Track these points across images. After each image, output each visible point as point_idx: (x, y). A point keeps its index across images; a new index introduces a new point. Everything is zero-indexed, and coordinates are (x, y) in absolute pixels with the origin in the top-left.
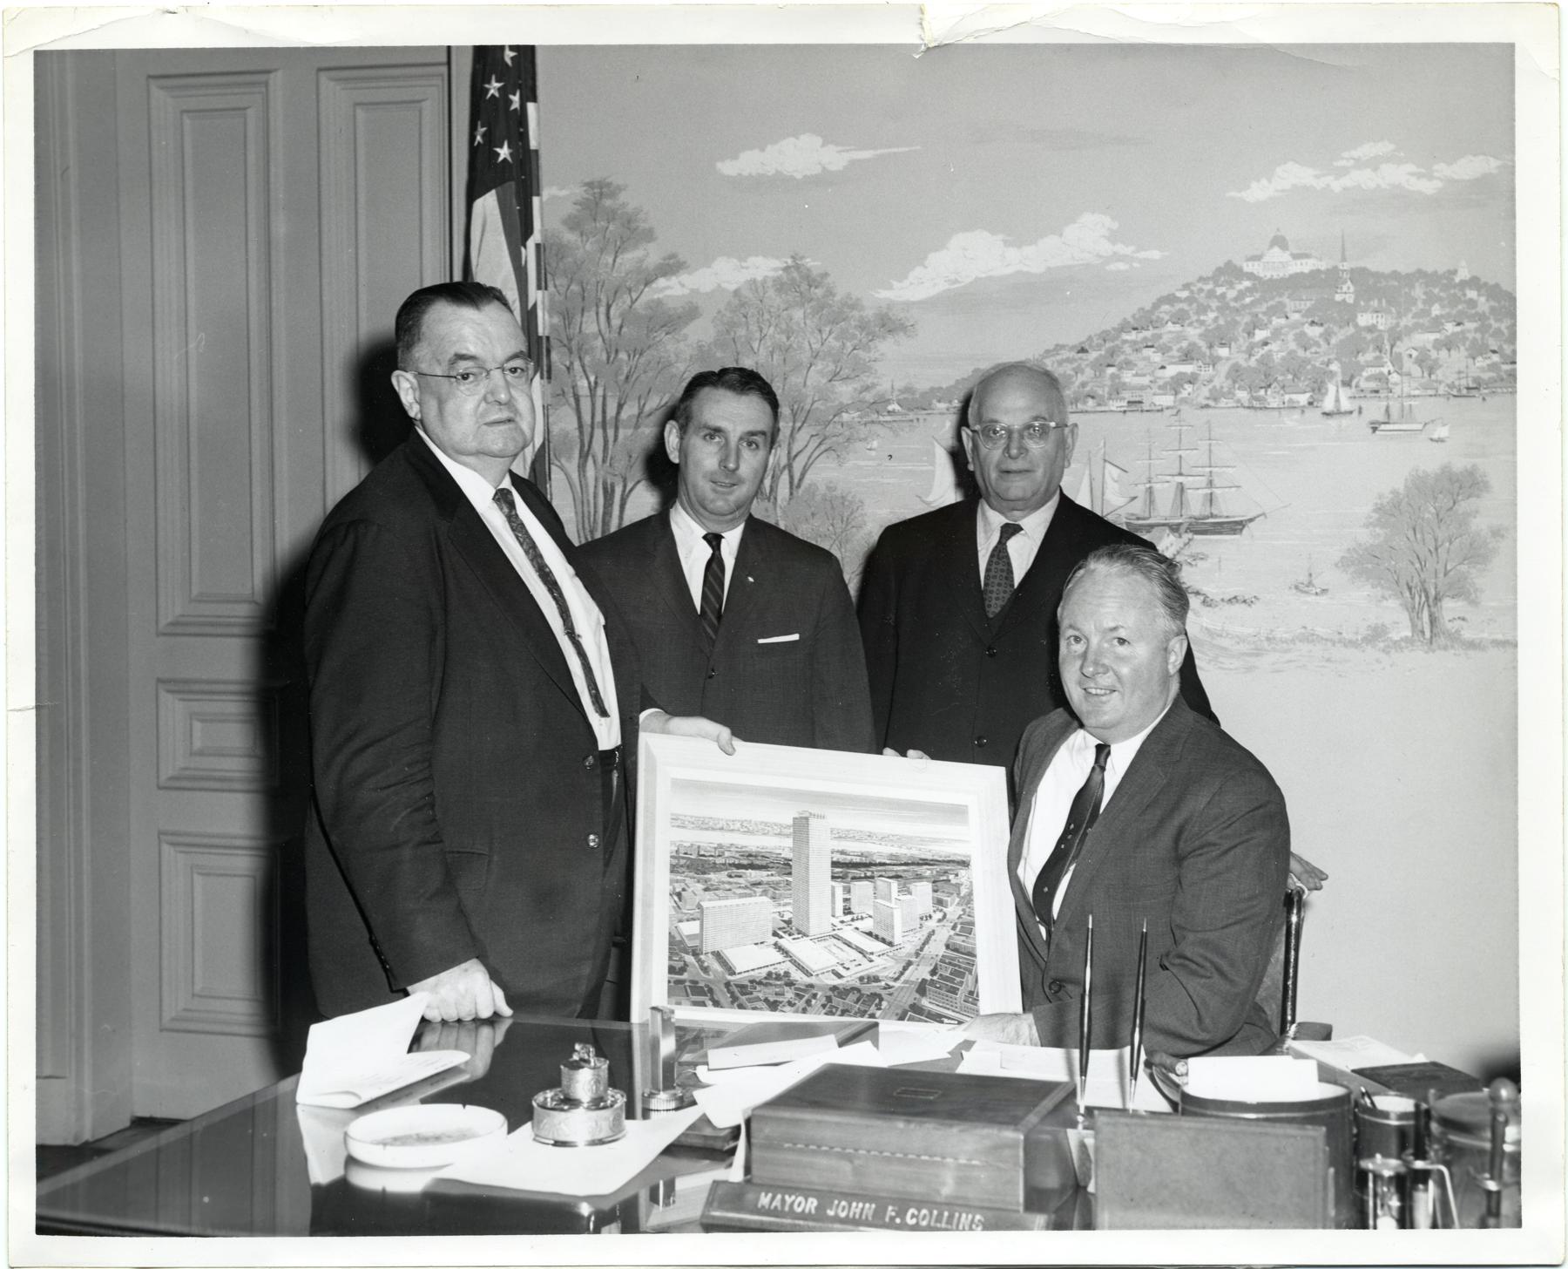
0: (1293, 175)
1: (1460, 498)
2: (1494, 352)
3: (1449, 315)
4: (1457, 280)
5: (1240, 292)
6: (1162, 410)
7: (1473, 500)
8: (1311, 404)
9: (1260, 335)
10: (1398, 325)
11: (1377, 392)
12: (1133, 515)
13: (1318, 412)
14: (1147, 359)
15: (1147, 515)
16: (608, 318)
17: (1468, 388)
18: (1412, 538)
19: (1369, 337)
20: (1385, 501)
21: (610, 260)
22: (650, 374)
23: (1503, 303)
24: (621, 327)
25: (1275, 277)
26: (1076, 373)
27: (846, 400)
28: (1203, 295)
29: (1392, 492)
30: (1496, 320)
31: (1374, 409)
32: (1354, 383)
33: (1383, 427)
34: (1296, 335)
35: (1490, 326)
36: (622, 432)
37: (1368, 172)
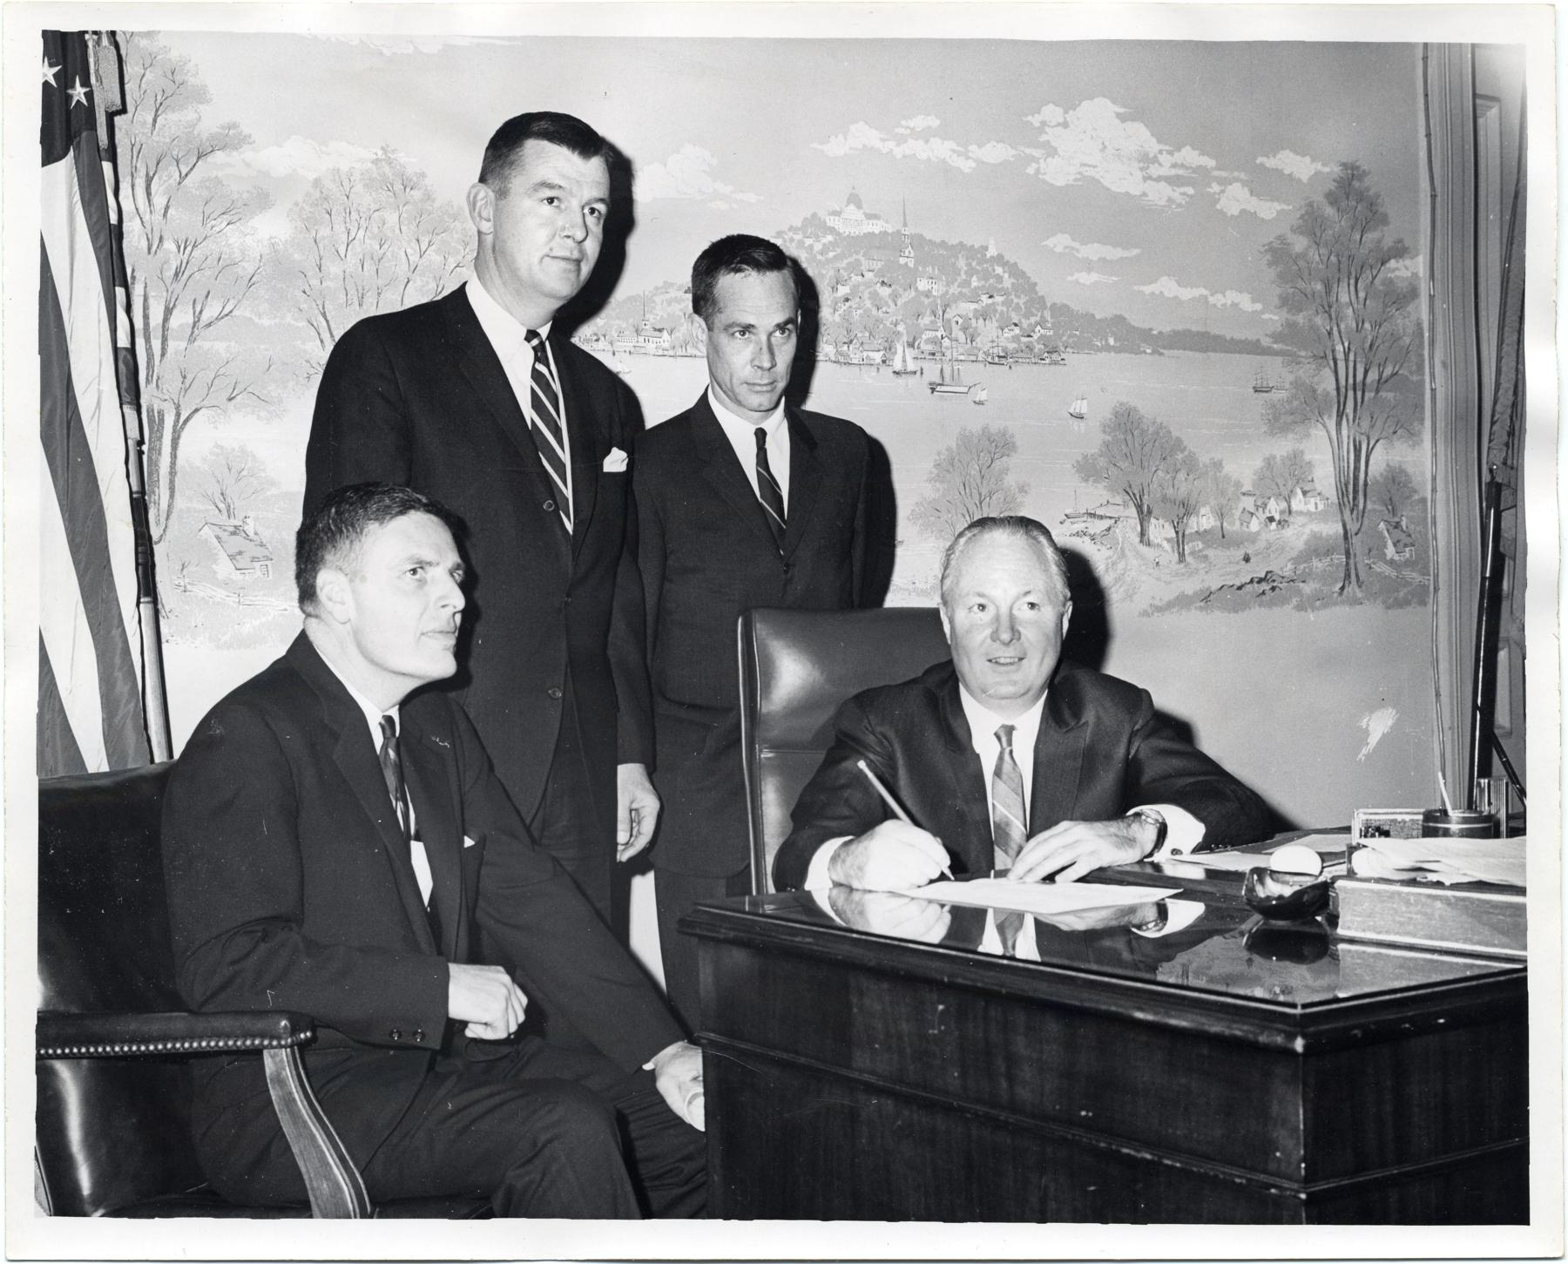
0: (865, 135)
1: (996, 456)
2: (1016, 325)
3: (984, 286)
4: (988, 256)
5: (824, 245)
7: (1005, 458)
8: (884, 362)
9: (843, 291)
10: (947, 292)
11: (934, 354)
13: (890, 370)
16: (149, 194)
17: (999, 357)
18: (963, 493)
19: (926, 301)
20: (943, 457)
21: (150, 119)
22: (208, 273)
23: (1020, 281)
24: (167, 208)
25: (852, 234)
28: (793, 244)
29: (947, 450)
30: (1016, 296)
31: (932, 372)
32: (916, 344)
33: (939, 388)
34: (870, 293)
35: (1012, 300)
36: (171, 345)
37: (921, 142)
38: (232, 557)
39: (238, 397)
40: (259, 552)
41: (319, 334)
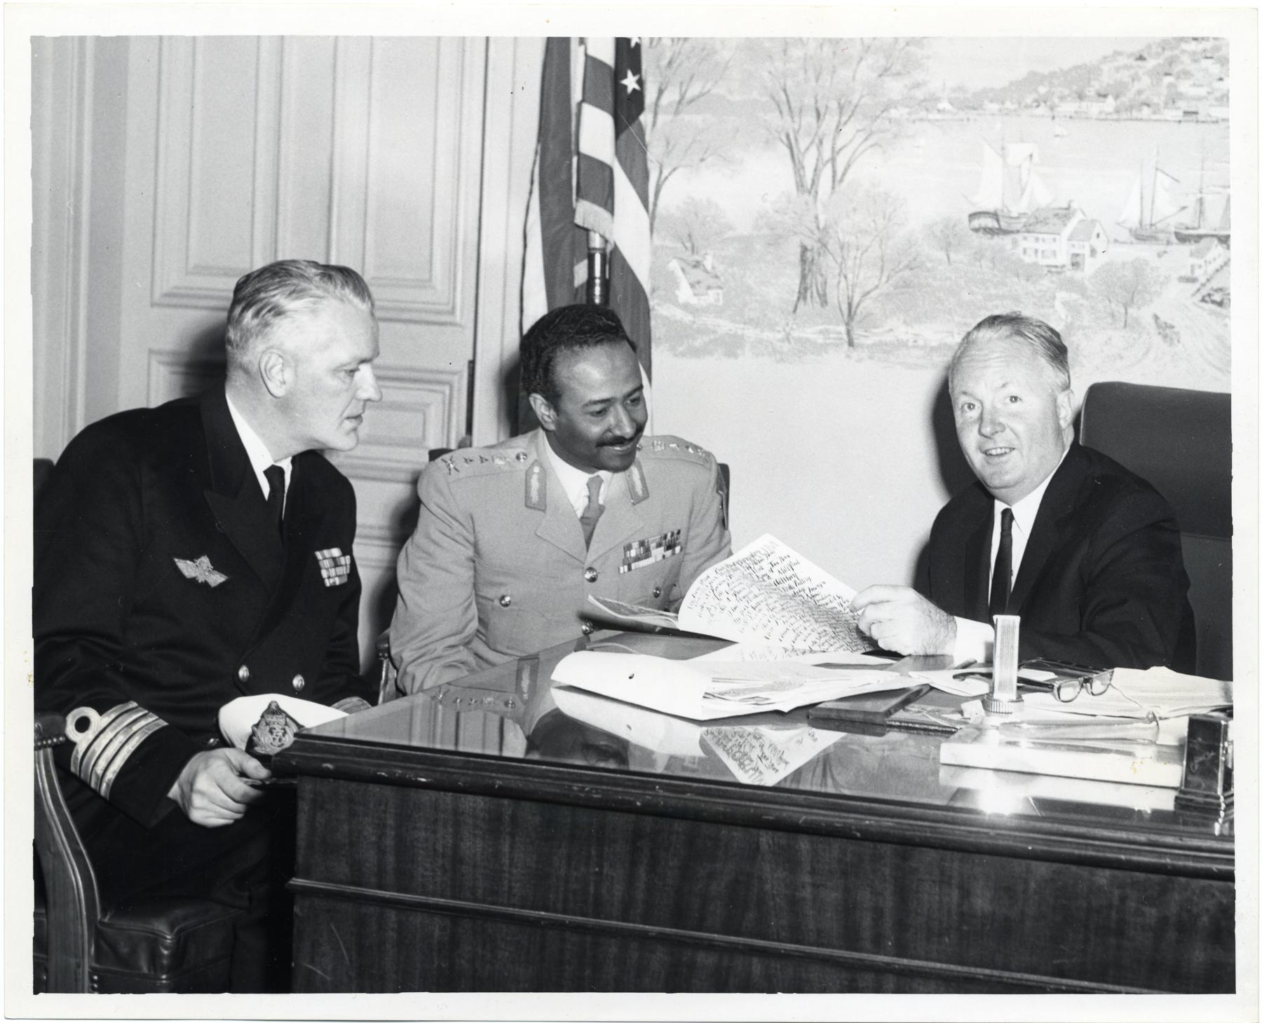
6: (1217, 122)
12: (1182, 224)
14: (1206, 70)
15: (1196, 225)
26: (1133, 80)
27: (895, 96)
36: (661, 118)
38: (692, 286)
39: (709, 160)
40: (712, 281)
41: (779, 106)
